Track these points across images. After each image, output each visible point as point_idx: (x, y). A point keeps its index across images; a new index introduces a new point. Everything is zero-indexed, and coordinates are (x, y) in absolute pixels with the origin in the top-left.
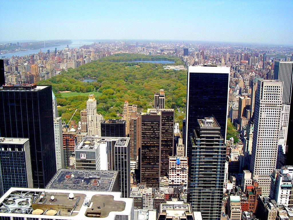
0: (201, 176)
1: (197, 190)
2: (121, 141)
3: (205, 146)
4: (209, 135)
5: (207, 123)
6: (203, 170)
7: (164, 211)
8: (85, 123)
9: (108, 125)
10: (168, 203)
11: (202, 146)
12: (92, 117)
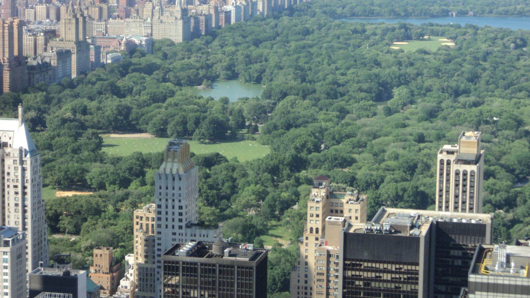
12: (174, 237)
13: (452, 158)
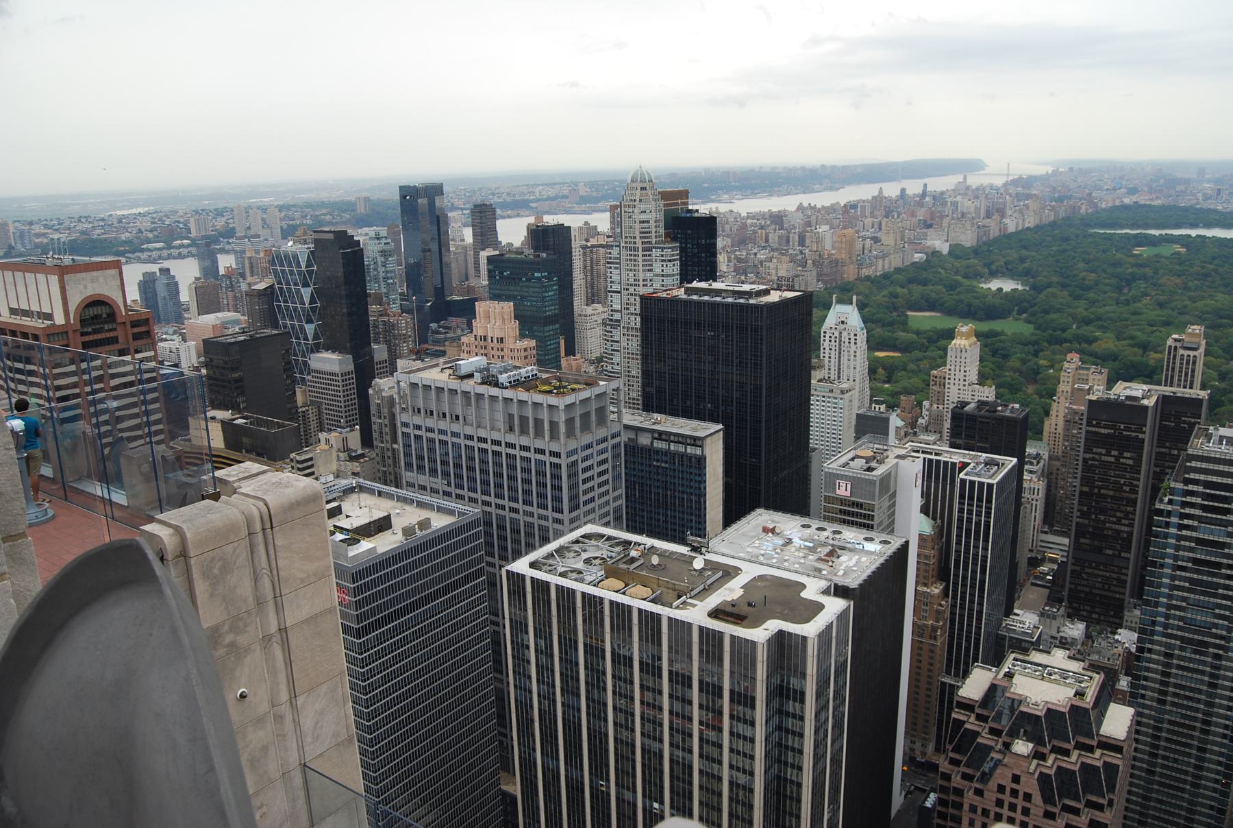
0: (1179, 603)
1: (1160, 643)
2: (986, 464)
3: (1198, 512)
4: (1215, 479)
5: (1221, 438)
6: (1187, 585)
7: (1009, 675)
8: (941, 407)
9: (971, 418)
10: (1036, 657)
11: (1187, 511)
13: (1178, 344)
